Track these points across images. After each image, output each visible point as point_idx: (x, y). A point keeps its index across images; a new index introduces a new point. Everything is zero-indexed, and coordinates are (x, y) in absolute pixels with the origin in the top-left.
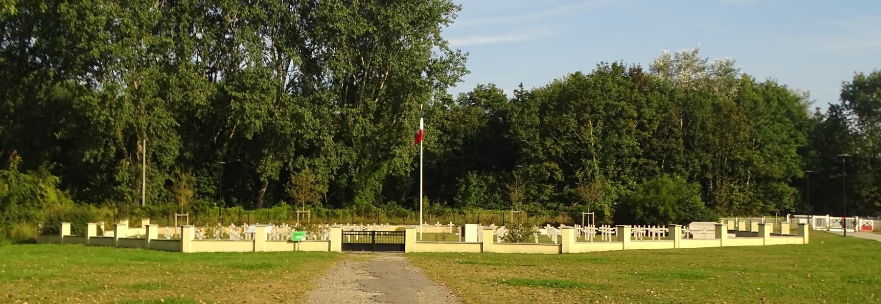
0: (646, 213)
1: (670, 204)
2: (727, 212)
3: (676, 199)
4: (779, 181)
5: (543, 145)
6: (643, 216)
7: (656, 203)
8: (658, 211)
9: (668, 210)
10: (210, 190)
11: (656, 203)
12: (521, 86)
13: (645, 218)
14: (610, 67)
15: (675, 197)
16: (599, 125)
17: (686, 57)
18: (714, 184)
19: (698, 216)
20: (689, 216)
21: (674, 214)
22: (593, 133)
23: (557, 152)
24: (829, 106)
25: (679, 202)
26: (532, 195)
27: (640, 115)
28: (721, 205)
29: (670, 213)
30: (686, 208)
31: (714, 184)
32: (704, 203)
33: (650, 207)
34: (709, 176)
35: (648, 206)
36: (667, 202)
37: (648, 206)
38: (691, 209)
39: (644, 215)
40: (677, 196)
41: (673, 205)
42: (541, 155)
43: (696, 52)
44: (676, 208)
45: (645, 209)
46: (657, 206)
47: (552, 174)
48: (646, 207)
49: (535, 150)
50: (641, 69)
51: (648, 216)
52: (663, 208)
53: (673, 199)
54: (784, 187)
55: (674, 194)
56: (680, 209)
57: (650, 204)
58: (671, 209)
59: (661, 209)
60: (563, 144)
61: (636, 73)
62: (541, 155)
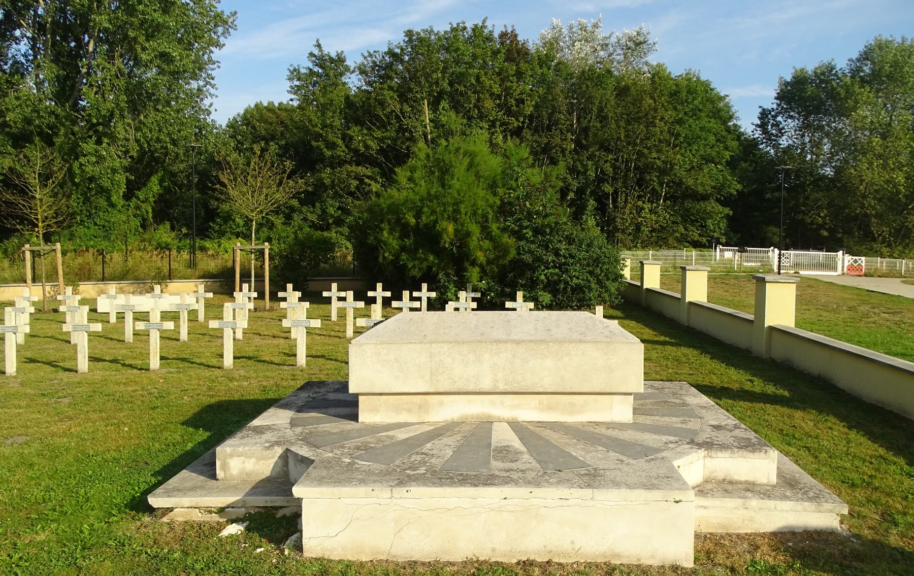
1: (475, 213)
2: (632, 241)
4: (705, 198)
6: (397, 256)
7: (433, 212)
8: (439, 235)
9: (468, 234)
11: (433, 212)
12: (319, 46)
13: (404, 256)
14: (469, 30)
15: (495, 194)
16: (443, 109)
17: (583, 28)
18: (615, 201)
19: (557, 253)
20: (530, 252)
21: (487, 244)
23: (367, 147)
24: (760, 110)
25: (505, 210)
26: (332, 216)
27: (508, 92)
28: (623, 231)
29: (474, 242)
30: (522, 227)
31: (615, 201)
32: (600, 228)
33: (418, 223)
34: (608, 188)
35: (413, 221)
37: (413, 221)
38: (537, 231)
39: (403, 249)
40: (501, 191)
41: (485, 217)
42: (341, 151)
43: (596, 26)
45: (404, 230)
46: (436, 222)
47: (361, 181)
49: (332, 146)
50: (516, 36)
52: (451, 228)
53: (482, 198)
54: (713, 206)
56: (504, 230)
57: (418, 216)
58: (475, 229)
59: (445, 230)
60: (378, 134)
61: (509, 37)
62: (341, 151)
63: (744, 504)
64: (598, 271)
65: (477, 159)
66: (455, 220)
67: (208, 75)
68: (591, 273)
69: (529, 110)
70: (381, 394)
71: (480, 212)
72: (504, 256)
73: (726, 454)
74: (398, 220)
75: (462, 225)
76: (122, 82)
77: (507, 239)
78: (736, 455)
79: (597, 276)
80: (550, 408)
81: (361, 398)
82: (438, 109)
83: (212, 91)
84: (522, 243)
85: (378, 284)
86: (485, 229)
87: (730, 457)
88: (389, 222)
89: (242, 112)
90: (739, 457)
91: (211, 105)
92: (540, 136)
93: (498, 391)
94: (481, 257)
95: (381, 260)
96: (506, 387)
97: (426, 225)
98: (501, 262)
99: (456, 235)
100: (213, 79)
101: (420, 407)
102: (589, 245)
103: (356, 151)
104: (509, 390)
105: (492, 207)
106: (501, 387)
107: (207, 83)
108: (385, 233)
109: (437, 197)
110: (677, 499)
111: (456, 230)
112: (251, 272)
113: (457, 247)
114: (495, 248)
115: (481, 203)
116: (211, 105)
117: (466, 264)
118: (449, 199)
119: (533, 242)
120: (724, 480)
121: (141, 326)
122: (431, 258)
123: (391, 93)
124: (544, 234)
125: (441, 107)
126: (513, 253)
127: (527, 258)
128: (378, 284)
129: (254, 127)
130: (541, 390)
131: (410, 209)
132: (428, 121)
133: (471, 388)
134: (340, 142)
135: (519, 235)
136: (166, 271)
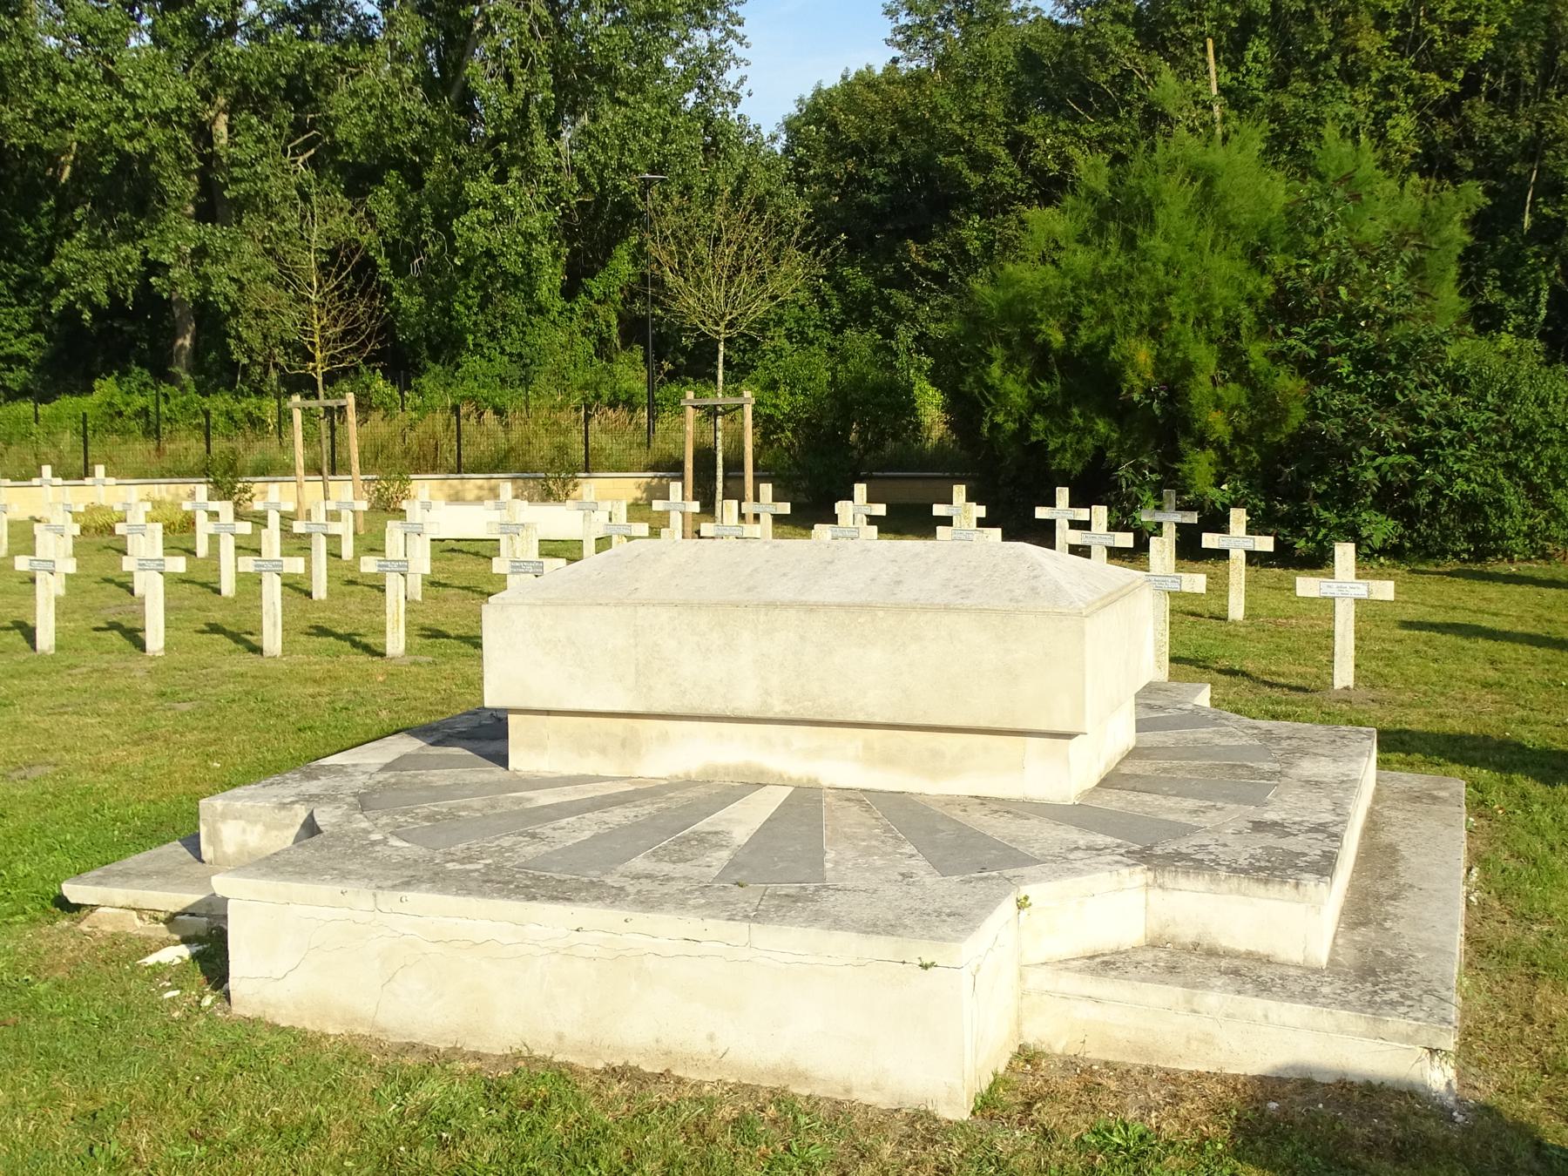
0: (1046, 388)
1: (1204, 319)
3: (1269, 289)
5: (1016, 144)
9: (1187, 369)
10: (20, 347)
11: (1106, 317)
13: (1039, 424)
15: (1264, 270)
16: (1256, 59)
19: (1411, 415)
21: (1234, 392)
22: (1224, 91)
29: (1201, 388)
35: (1057, 338)
36: (1173, 305)
38: (1367, 361)
39: (1038, 405)
40: (1278, 261)
41: (1232, 325)
42: (1005, 173)
44: (1256, 352)
45: (1042, 360)
46: (1111, 339)
48: (1046, 346)
49: (982, 163)
51: (1054, 411)
52: (1143, 354)
55: (1256, 257)
56: (1277, 358)
57: (1071, 323)
58: (1205, 357)
62: (1005, 173)
63: (1189, 1001)
64: (1528, 462)
65: (1221, 186)
66: (1155, 333)
67: (731, 15)
68: (1510, 468)
69: (1478, 48)
70: (548, 713)
71: (1219, 313)
72: (1276, 424)
73: (1200, 883)
74: (1028, 337)
75: (1174, 345)
76: (540, 48)
77: (1288, 383)
78: (1224, 887)
79: (1526, 477)
80: (889, 760)
81: (513, 720)
82: (1241, 61)
83: (739, 51)
84: (1320, 392)
85: (956, 488)
86: (1231, 357)
87: (1209, 891)
88: (1006, 342)
89: (808, 95)
90: (1231, 891)
91: (742, 80)
92: (1513, 116)
93: (770, 715)
94: (1218, 424)
95: (985, 430)
96: (788, 708)
97: (1088, 347)
98: (1269, 437)
99: (1157, 373)
100: (740, 24)
101: (623, 745)
102: (1508, 395)
103: (1038, 173)
104: (793, 715)
105: (1250, 301)
106: (778, 709)
107: (730, 33)
108: (995, 371)
109: (1113, 278)
110: (927, 961)
111: (1159, 359)
112: (715, 456)
113: (1163, 401)
114: (1254, 403)
115: (1220, 292)
116: (742, 80)
117: (1183, 444)
118: (1143, 284)
119: (1354, 388)
120: (1196, 946)
121: (248, 564)
122: (1101, 426)
123: (1121, 29)
124: (1381, 366)
125: (1249, 55)
126: (1297, 416)
127: (1333, 428)
128: (956, 488)
129: (833, 126)
130: (861, 718)
131: (1052, 311)
132: (1215, 92)
133: (716, 708)
134: (1002, 153)
135: (1314, 370)
136: (578, 454)
